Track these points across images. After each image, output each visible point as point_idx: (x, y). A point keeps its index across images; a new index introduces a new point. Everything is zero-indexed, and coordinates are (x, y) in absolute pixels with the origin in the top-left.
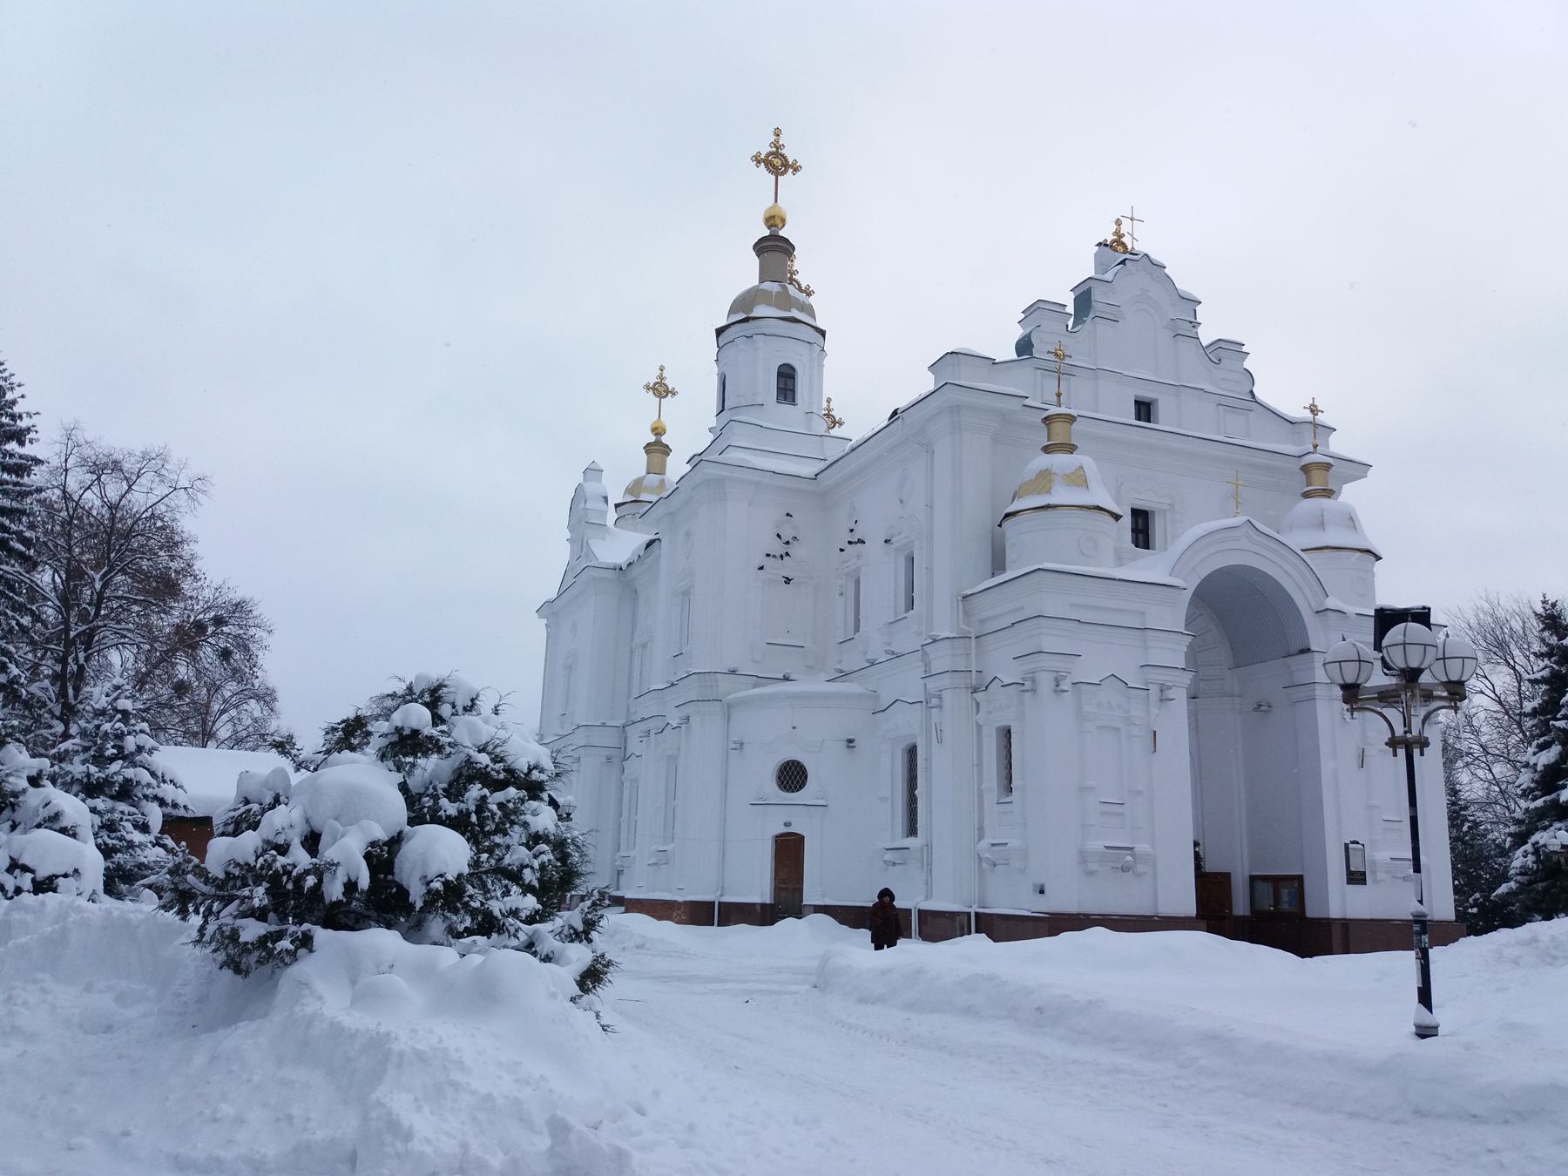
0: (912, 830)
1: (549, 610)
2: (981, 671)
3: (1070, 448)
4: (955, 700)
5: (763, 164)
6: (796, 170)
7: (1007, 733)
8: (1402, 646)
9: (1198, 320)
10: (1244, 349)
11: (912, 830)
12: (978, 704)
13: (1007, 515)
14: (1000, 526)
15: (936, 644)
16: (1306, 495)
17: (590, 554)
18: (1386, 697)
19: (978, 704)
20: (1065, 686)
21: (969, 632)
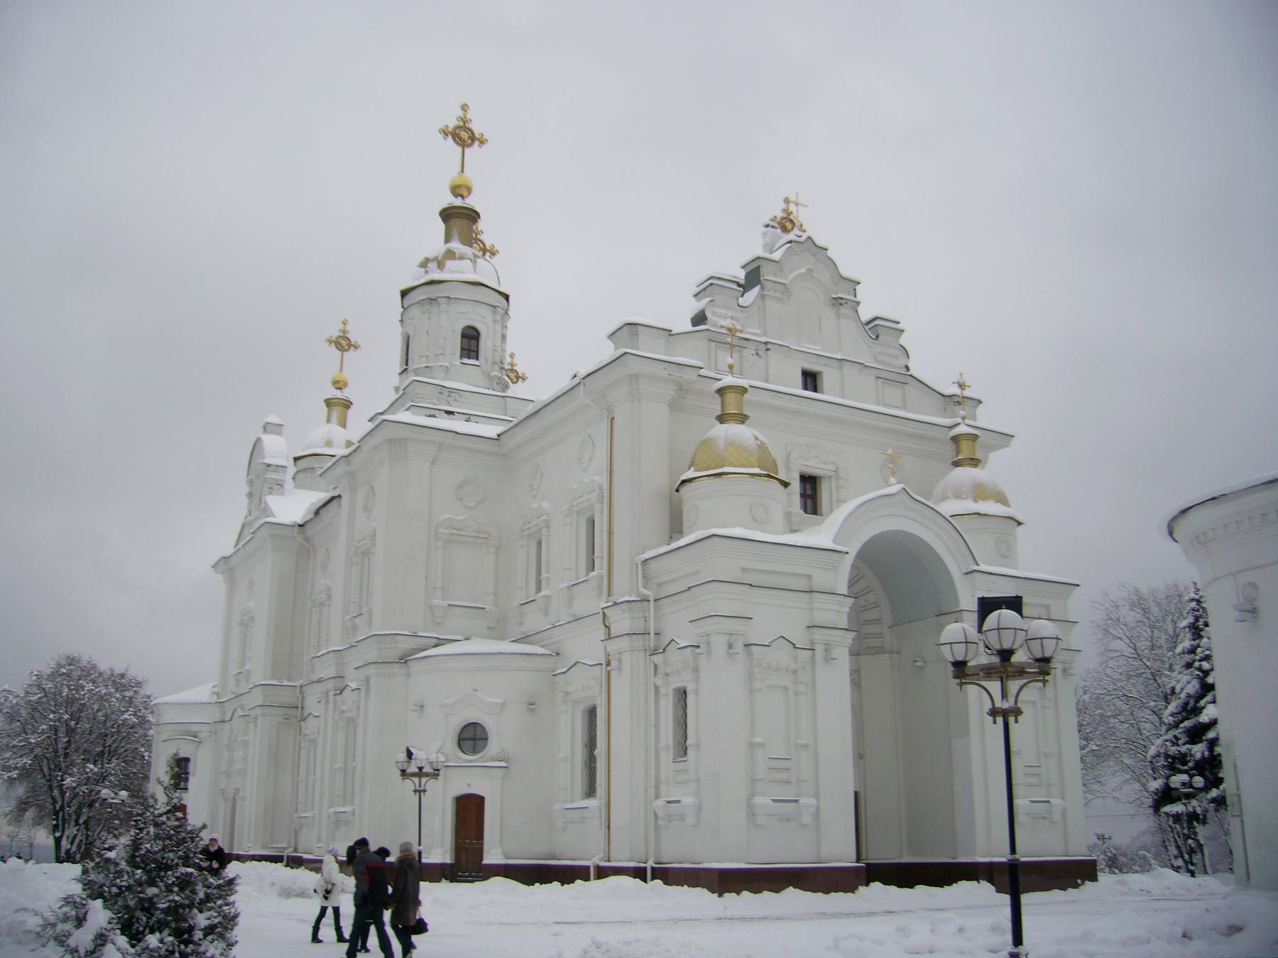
0: (591, 791)
1: (224, 564)
2: (658, 634)
3: (742, 418)
5: (450, 137)
6: (482, 142)
7: (682, 694)
8: (997, 631)
9: (858, 299)
10: (899, 326)
11: (591, 791)
12: (656, 666)
13: (684, 482)
14: (677, 491)
15: (616, 607)
16: (957, 464)
17: (266, 511)
18: (988, 672)
19: (656, 666)
20: (739, 647)
21: (648, 596)
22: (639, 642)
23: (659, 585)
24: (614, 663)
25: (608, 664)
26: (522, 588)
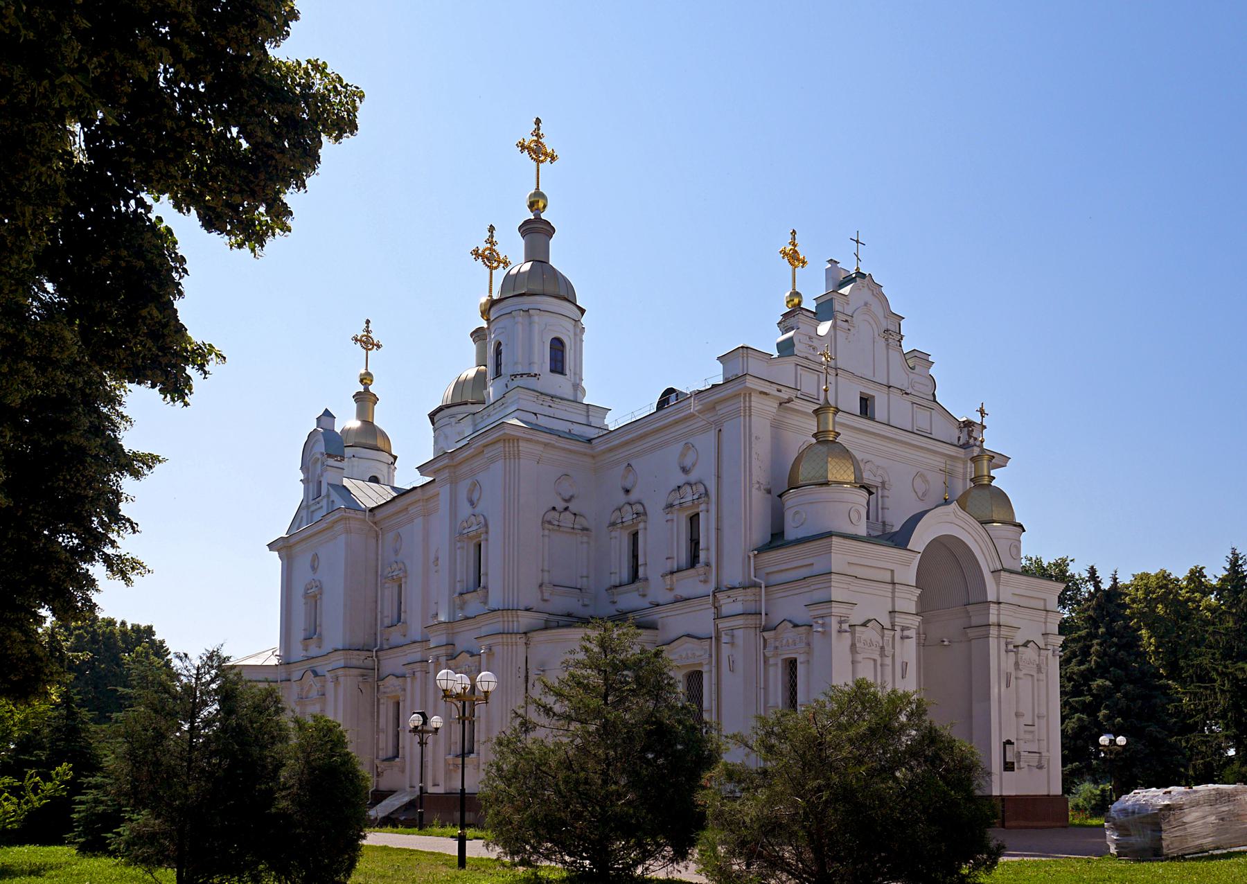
4: (743, 638)
7: (792, 665)
19: (765, 640)
22: (751, 620)
23: (768, 574)
24: (725, 638)
25: (718, 639)
26: (615, 573)
